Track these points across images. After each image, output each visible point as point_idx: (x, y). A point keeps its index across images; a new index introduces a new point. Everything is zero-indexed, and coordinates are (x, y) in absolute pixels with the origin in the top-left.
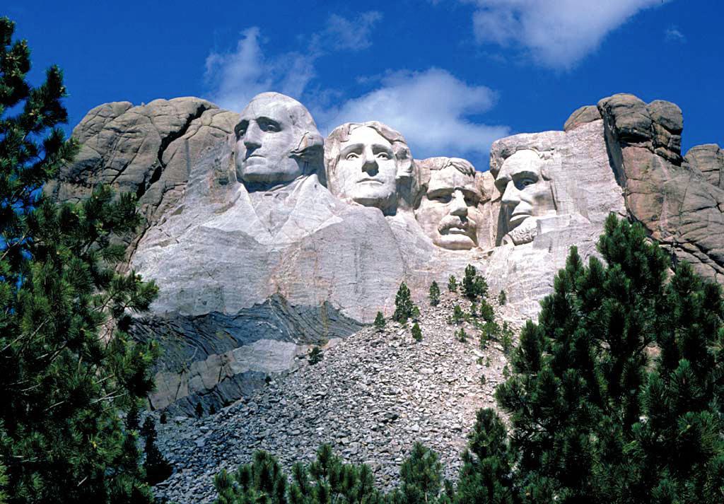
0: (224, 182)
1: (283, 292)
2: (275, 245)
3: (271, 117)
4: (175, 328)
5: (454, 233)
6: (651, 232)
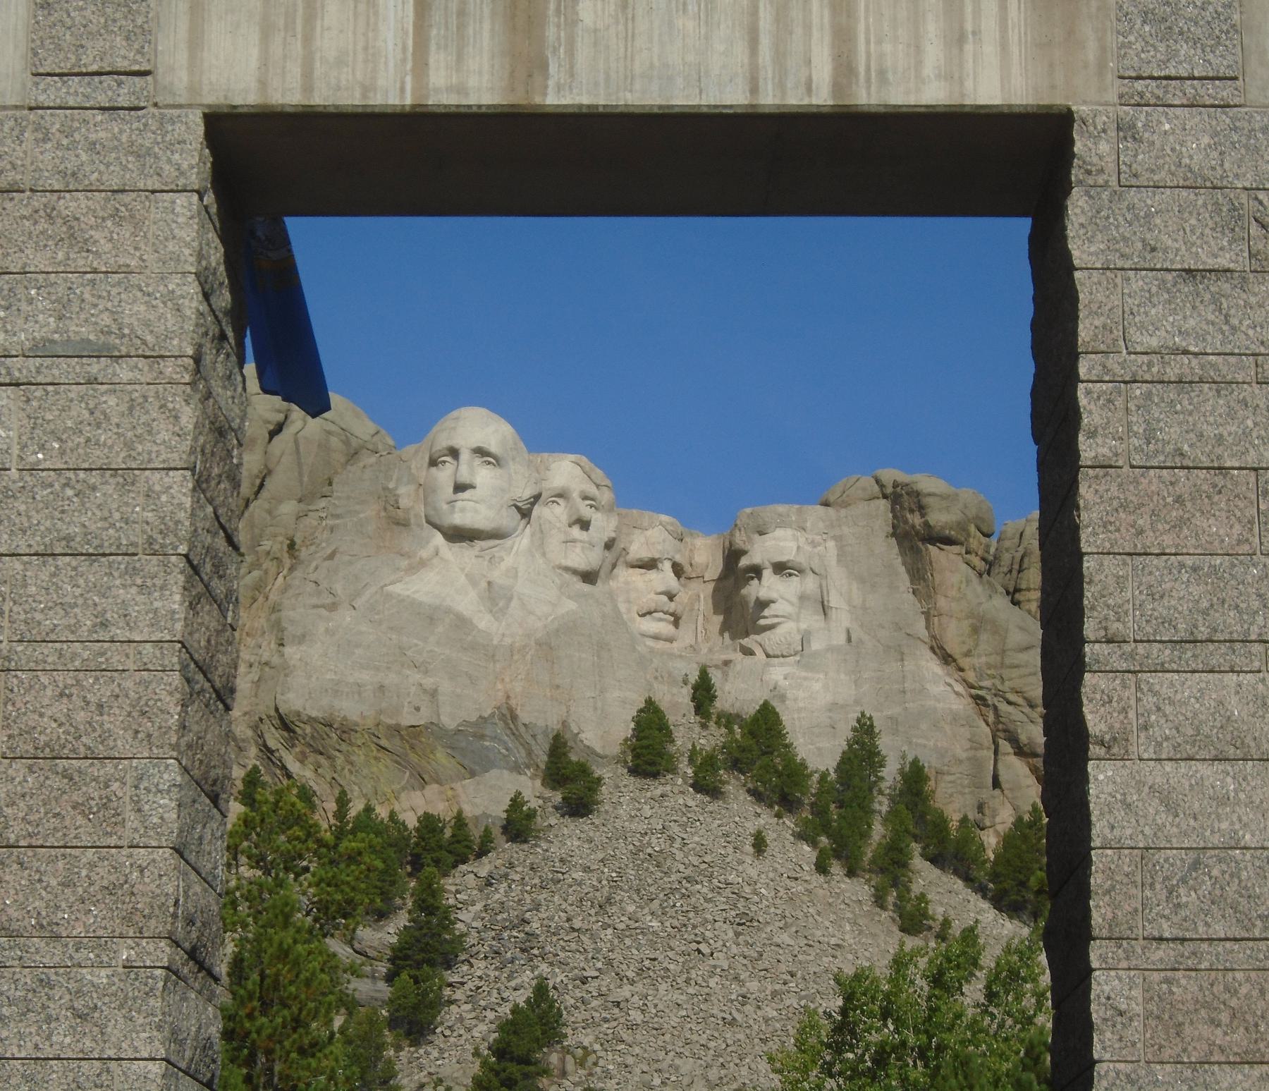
0: (403, 524)
1: (513, 702)
2: (503, 635)
3: (493, 449)
4: (375, 740)
5: (661, 620)
6: (962, 670)
